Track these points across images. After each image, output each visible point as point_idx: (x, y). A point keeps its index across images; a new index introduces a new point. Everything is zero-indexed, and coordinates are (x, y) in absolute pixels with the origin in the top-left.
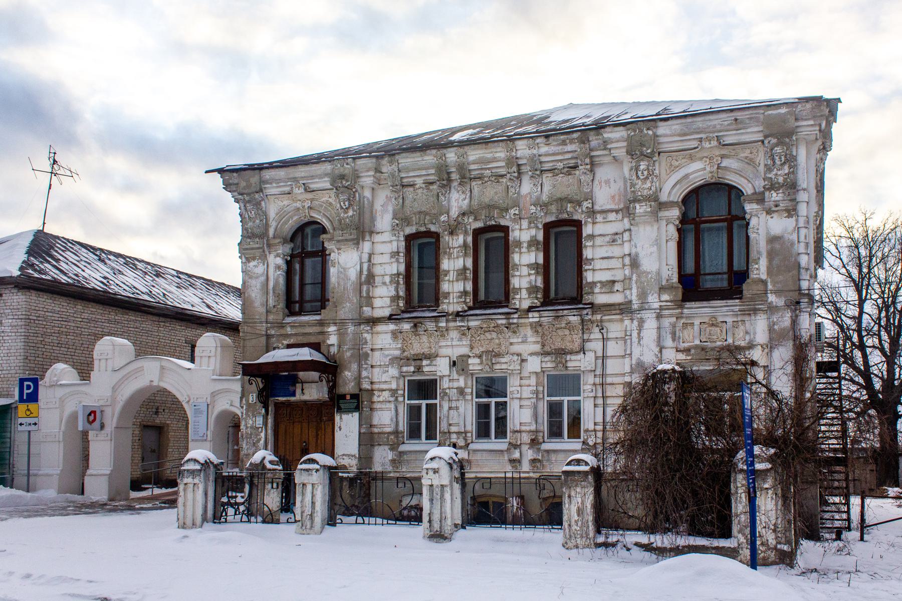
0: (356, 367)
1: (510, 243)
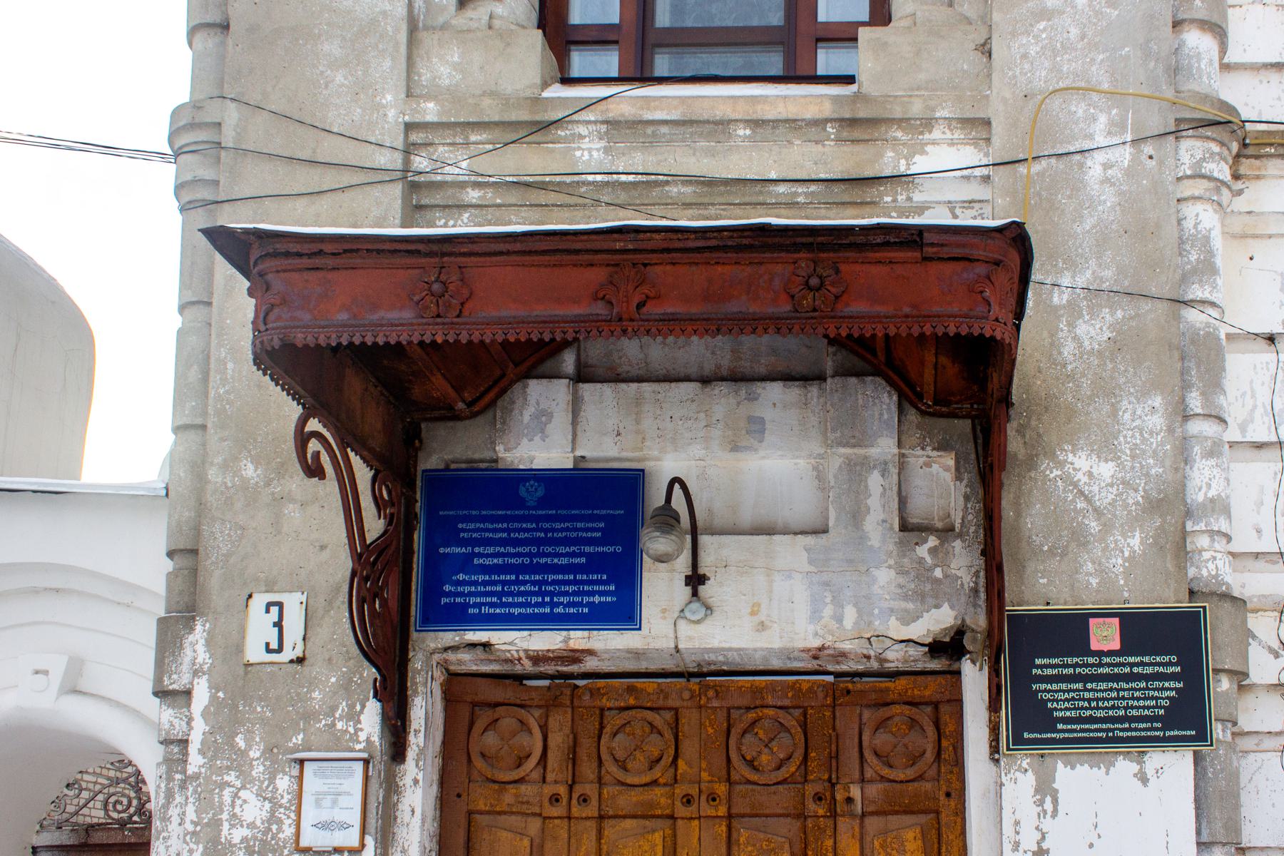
0: (1157, 421)
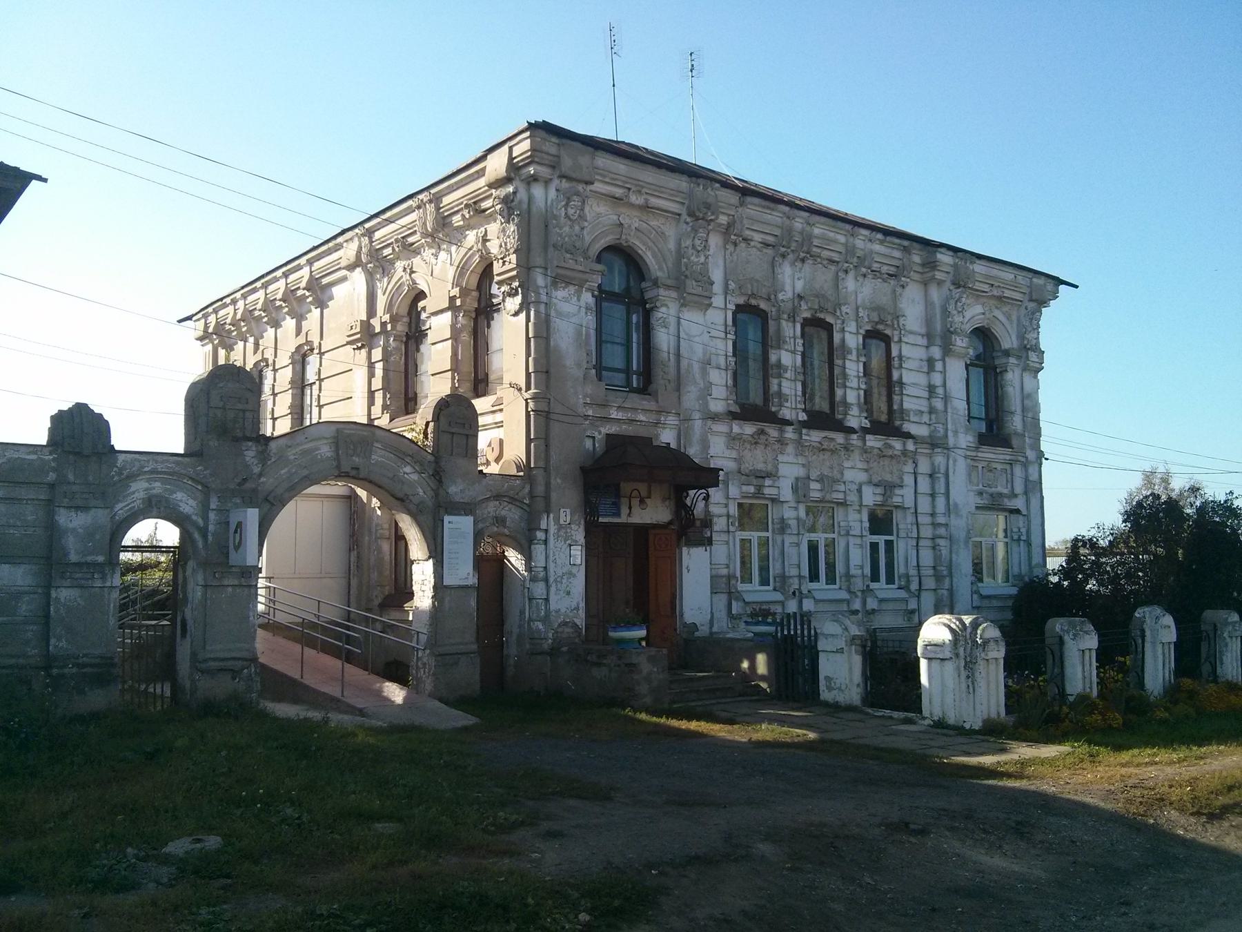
1: (835, 346)
